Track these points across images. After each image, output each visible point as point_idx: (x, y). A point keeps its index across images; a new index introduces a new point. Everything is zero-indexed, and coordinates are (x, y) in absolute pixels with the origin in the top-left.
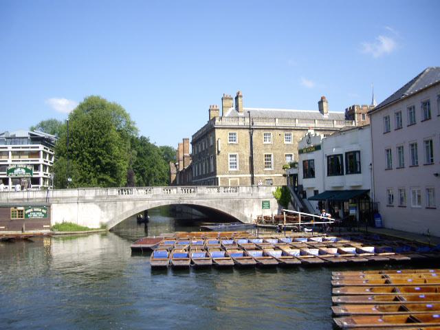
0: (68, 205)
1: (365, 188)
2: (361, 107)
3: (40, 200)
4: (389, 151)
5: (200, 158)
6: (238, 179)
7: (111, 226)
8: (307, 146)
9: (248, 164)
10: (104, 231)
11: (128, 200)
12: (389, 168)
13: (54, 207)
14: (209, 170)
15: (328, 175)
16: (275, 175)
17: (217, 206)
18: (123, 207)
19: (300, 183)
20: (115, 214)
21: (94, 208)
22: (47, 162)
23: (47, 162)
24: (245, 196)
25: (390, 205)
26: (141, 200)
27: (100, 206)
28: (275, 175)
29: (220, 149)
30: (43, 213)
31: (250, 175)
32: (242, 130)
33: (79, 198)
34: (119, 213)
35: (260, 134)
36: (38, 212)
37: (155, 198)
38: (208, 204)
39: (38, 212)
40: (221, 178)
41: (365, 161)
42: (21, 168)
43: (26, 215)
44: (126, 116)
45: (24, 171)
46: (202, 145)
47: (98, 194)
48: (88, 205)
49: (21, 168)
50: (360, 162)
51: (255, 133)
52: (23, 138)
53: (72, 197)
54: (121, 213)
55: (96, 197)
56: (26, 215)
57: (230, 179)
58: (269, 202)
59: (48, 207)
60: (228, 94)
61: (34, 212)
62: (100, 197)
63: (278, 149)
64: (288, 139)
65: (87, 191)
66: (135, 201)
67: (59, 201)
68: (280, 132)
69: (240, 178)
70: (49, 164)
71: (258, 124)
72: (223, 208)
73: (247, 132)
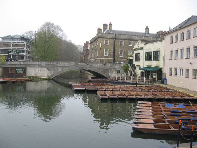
0: (34, 68)
1: (161, 67)
2: (163, 32)
4: (171, 51)
5: (92, 50)
6: (108, 60)
10: (50, 80)
11: (60, 67)
12: (171, 59)
13: (28, 68)
14: (96, 56)
15: (146, 61)
18: (57, 69)
19: (134, 63)
20: (54, 72)
21: (45, 69)
22: (28, 49)
23: (28, 49)
24: (110, 67)
25: (171, 74)
26: (65, 67)
27: (47, 69)
29: (101, 47)
32: (110, 39)
33: (39, 65)
34: (56, 72)
35: (118, 41)
37: (71, 66)
38: (94, 70)
41: (162, 55)
42: (14, 51)
43: (16, 71)
44: (62, 31)
45: (15, 52)
46: (93, 45)
47: (47, 64)
48: (43, 68)
49: (14, 51)
51: (116, 41)
52: (17, 38)
53: (36, 64)
55: (46, 65)
56: (16, 71)
58: (120, 70)
59: (25, 69)
60: (106, 23)
61: (19, 70)
62: (48, 65)
64: (130, 44)
65: (42, 62)
66: (63, 67)
67: (30, 66)
68: (127, 41)
69: (109, 60)
70: (28, 50)
71: (118, 37)
73: (113, 40)
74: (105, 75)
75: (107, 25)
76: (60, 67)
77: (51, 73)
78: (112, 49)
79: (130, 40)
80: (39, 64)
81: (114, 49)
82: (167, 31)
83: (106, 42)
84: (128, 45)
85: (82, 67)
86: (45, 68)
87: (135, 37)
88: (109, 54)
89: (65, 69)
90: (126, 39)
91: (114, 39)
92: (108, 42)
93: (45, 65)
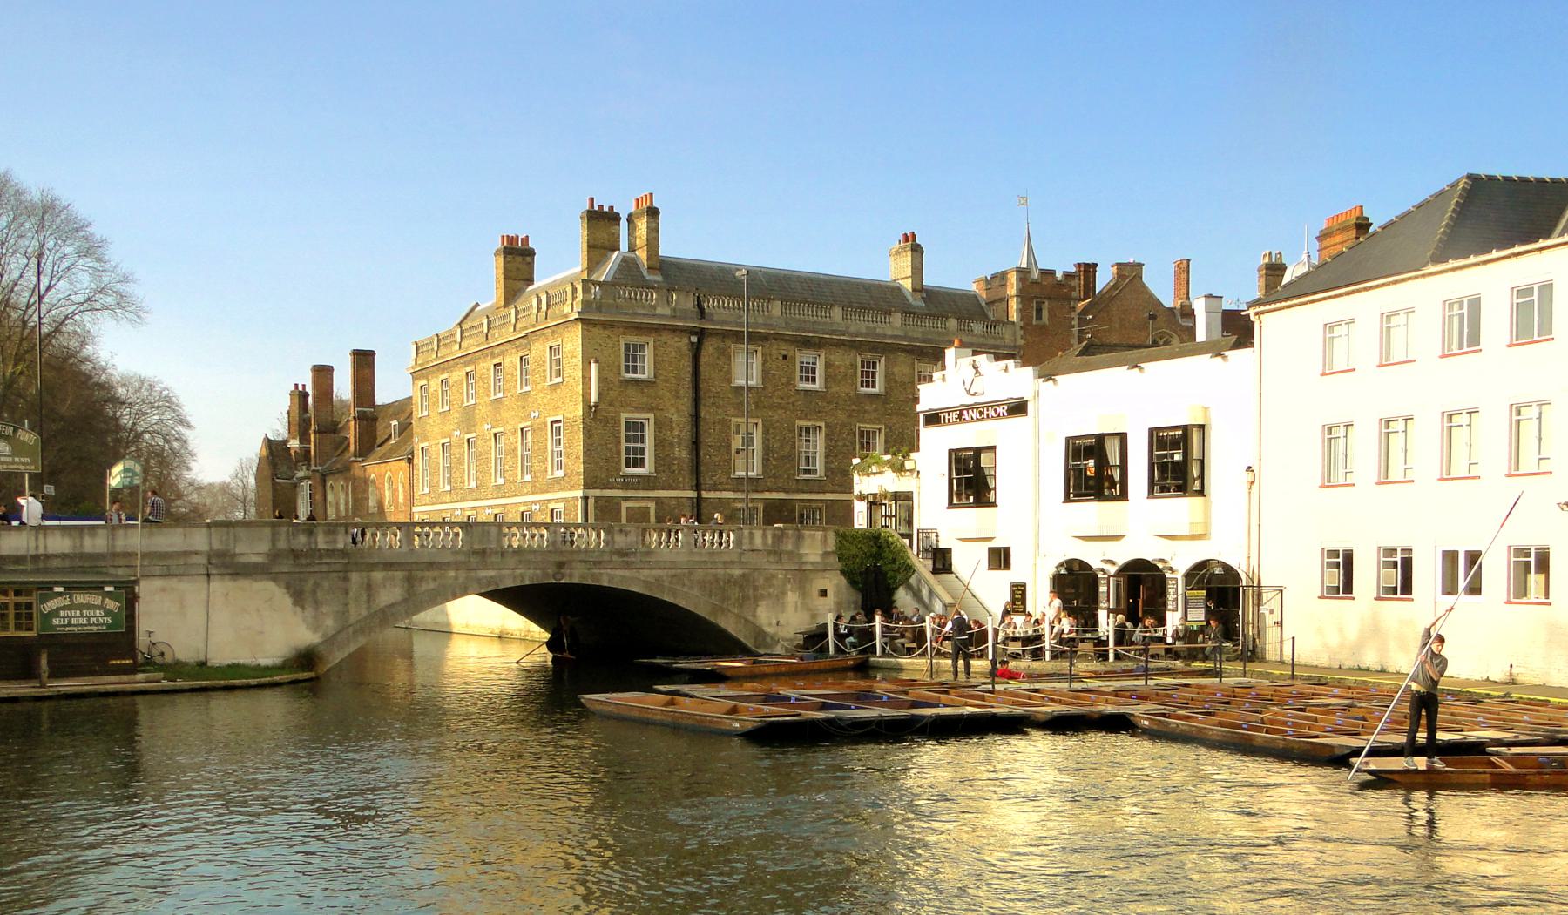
3: (67, 563)
6: (652, 506)
7: (337, 656)
8: (970, 400)
9: (682, 453)
11: (388, 566)
13: (145, 589)
16: (767, 495)
17: (674, 593)
18: (369, 587)
20: (343, 614)
27: (288, 587)
28: (767, 495)
30: (108, 613)
31: (705, 494)
32: (665, 337)
34: (357, 612)
36: (89, 607)
39: (89, 607)
40: (596, 498)
44: (91, 249)
47: (282, 544)
48: (244, 583)
50: (1202, 462)
51: (710, 349)
53: (186, 554)
54: (364, 612)
55: (275, 556)
57: (624, 505)
60: (605, 202)
63: (779, 406)
64: (809, 373)
68: (785, 349)
69: (657, 500)
72: (691, 600)
73: (682, 343)
74: (728, 624)
75: (613, 218)
76: (388, 566)
77: (315, 629)
78: (679, 415)
79: (805, 343)
80: (217, 546)
81: (696, 418)
82: (1059, 275)
83: (633, 361)
84: (790, 382)
85: (561, 565)
86: (270, 586)
87: (837, 313)
88: (657, 456)
89: (432, 585)
90: (778, 337)
91: (691, 331)
92: (649, 354)
93: (268, 555)
